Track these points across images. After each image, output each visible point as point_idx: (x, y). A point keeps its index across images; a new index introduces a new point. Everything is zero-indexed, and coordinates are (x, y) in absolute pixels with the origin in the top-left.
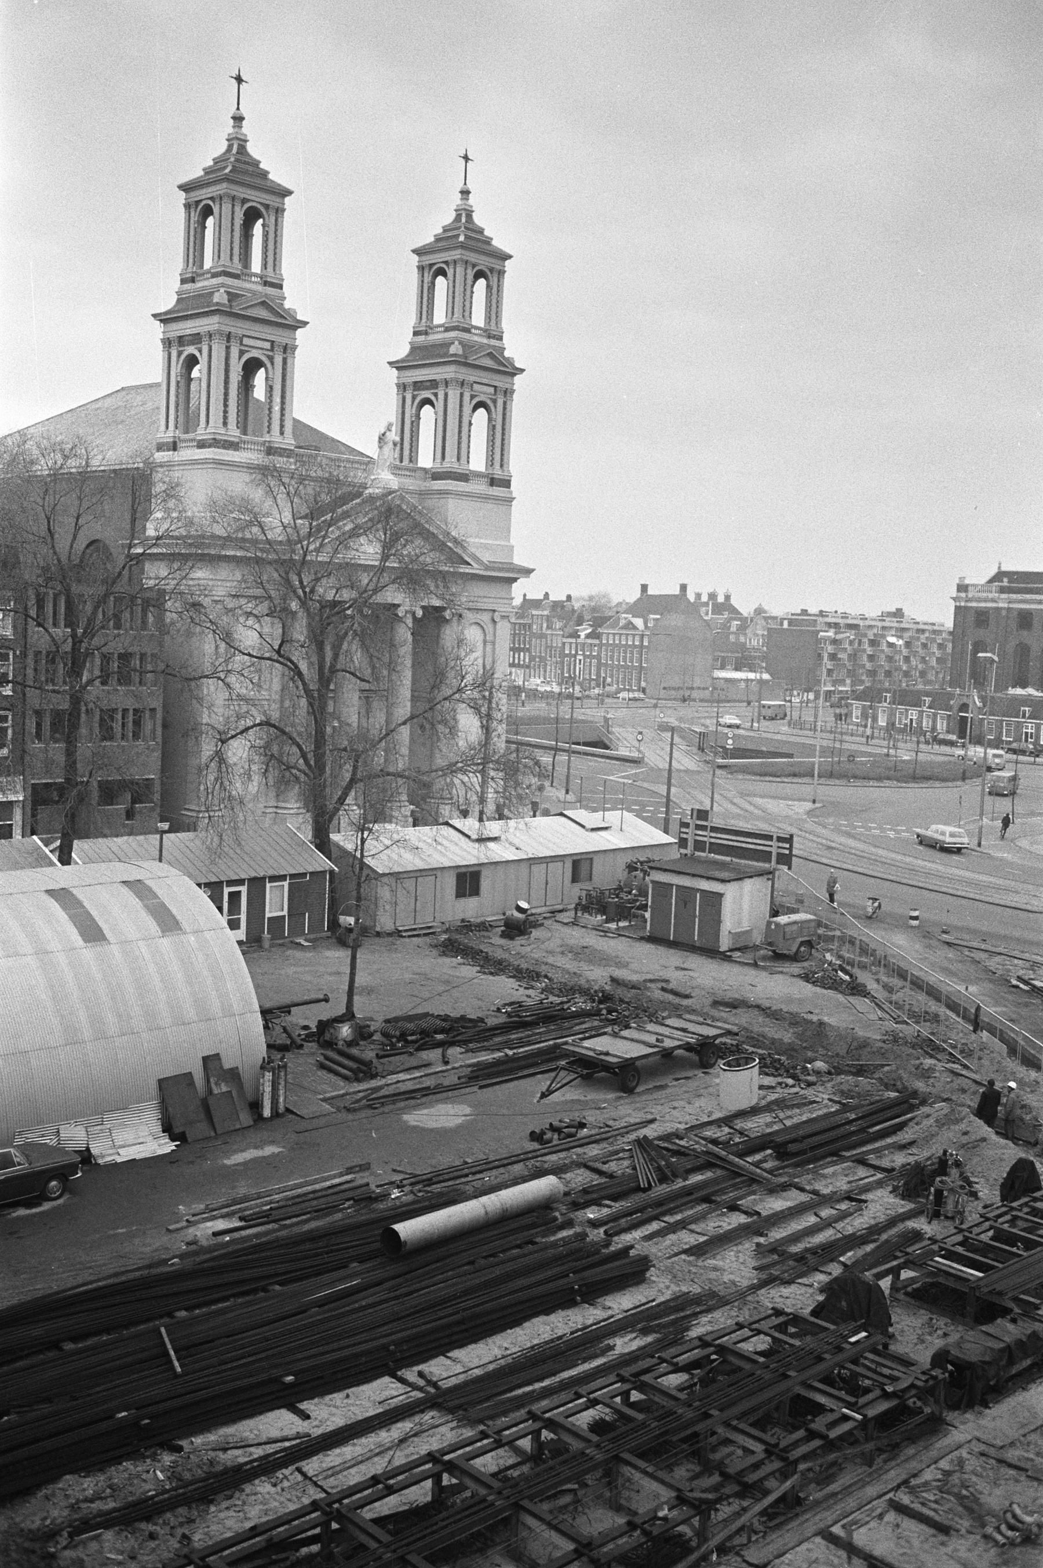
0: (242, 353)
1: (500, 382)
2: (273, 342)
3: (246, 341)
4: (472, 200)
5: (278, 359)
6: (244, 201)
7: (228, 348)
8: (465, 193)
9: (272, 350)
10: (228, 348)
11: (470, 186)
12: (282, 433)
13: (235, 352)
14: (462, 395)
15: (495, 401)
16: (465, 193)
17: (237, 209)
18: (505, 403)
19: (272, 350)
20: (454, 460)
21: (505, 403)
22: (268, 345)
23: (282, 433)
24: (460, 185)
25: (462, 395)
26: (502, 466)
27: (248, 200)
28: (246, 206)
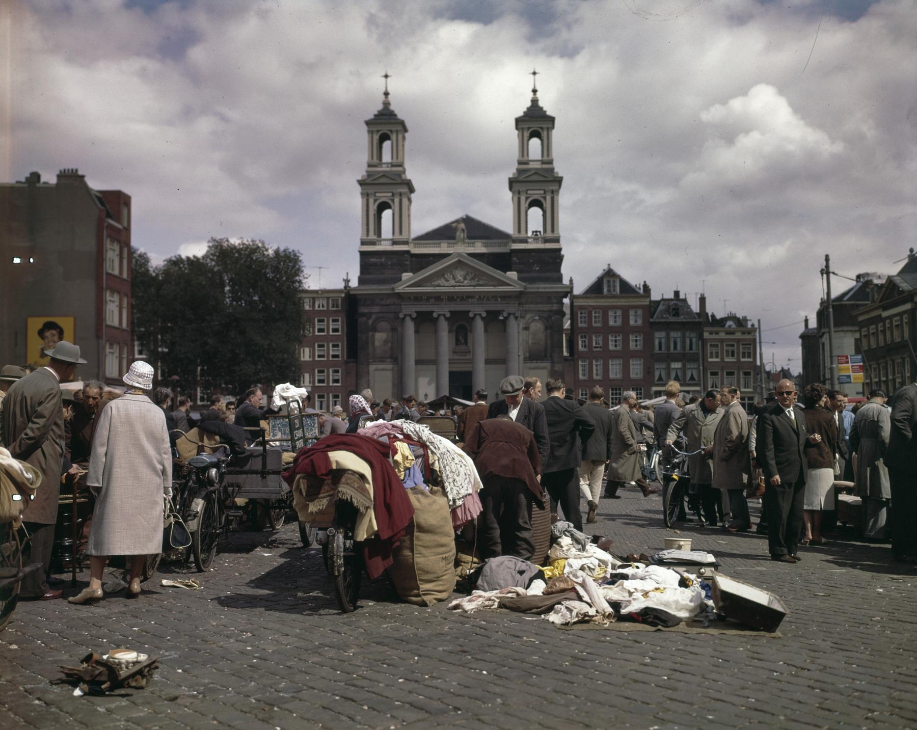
0: (375, 201)
4: (538, 95)
5: (397, 200)
6: (378, 131)
7: (368, 200)
8: (535, 91)
10: (368, 200)
11: (537, 88)
12: (401, 233)
13: (371, 201)
14: (519, 199)
15: (545, 198)
16: (535, 91)
23: (401, 233)
24: (532, 88)
25: (519, 199)
26: (553, 231)
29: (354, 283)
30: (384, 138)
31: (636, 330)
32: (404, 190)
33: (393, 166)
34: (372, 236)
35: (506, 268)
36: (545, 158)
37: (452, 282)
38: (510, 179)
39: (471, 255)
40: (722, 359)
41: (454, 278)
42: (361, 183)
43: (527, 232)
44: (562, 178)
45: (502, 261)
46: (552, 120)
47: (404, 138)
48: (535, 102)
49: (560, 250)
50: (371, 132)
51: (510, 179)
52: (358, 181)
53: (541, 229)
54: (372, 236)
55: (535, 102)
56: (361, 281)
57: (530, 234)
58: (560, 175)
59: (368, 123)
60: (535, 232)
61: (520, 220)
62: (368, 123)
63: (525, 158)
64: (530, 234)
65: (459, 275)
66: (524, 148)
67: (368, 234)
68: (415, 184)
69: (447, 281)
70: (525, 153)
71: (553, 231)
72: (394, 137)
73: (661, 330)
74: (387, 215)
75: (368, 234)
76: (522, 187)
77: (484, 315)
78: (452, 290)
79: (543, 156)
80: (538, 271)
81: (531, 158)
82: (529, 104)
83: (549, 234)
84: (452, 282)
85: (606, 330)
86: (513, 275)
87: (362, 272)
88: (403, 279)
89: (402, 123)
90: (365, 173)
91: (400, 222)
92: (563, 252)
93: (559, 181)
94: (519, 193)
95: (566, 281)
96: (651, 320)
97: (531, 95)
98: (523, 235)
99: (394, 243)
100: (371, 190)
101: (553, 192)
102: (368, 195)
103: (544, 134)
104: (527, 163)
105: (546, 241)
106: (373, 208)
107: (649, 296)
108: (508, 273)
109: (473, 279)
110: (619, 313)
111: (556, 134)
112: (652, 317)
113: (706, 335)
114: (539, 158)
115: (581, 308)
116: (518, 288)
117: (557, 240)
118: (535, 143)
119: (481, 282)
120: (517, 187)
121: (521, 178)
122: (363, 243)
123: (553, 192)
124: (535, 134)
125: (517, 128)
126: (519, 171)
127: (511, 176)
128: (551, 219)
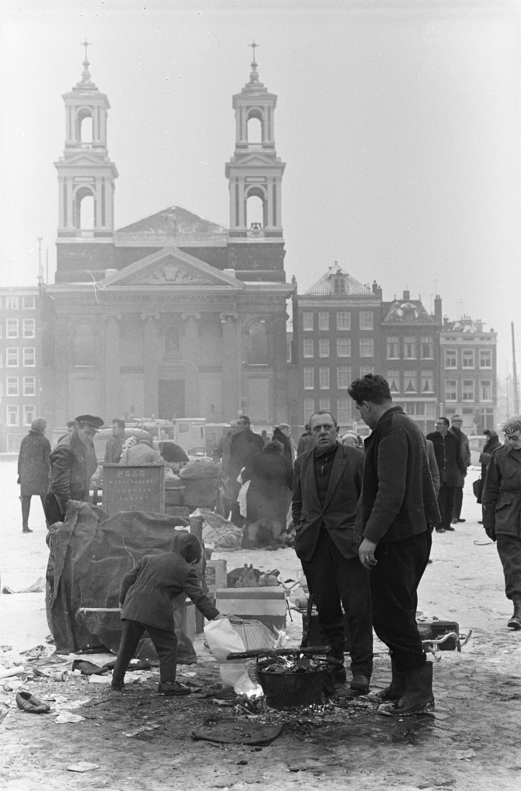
0: (74, 186)
1: (270, 174)
2: (94, 177)
3: (76, 179)
5: (99, 186)
6: (77, 107)
8: (254, 65)
9: (95, 181)
12: (103, 224)
14: (237, 187)
15: (266, 186)
16: (254, 65)
17: (73, 111)
18: (274, 187)
19: (95, 181)
20: (243, 225)
21: (274, 187)
22: (92, 179)
23: (103, 224)
25: (237, 187)
26: (275, 224)
27: (81, 106)
28: (78, 110)
29: (52, 281)
30: (83, 115)
31: (367, 335)
32: (107, 173)
33: (94, 147)
34: (71, 227)
35: (222, 265)
36: (267, 141)
37: (162, 280)
38: (227, 164)
39: (183, 249)
40: (460, 367)
41: (164, 275)
42: (58, 166)
43: (245, 225)
44: (285, 164)
45: (217, 257)
46: (274, 98)
47: (106, 115)
48: (254, 77)
49: (283, 244)
50: (69, 108)
51: (227, 164)
52: (54, 163)
53: (261, 221)
54: (71, 227)
55: (254, 77)
56: (58, 278)
57: (249, 226)
58: (283, 161)
59: (65, 97)
60: (255, 225)
61: (238, 211)
62: (65, 97)
63: (244, 141)
64: (249, 226)
65: (171, 271)
66: (242, 131)
67: (65, 225)
68: (119, 168)
69: (156, 278)
70: (244, 136)
71: (275, 224)
72: (95, 113)
73: (394, 335)
74: (87, 202)
75: (65, 225)
76: (242, 174)
77: (198, 317)
78: (163, 288)
79: (263, 139)
80: (258, 268)
81: (250, 141)
82: (248, 80)
83: (270, 227)
84: (162, 280)
85: (333, 336)
86: (230, 272)
87: (59, 268)
88: (107, 276)
89: (104, 98)
90: (62, 155)
91: (103, 211)
92: (285, 248)
93: (282, 167)
94: (237, 180)
95: (289, 280)
96: (383, 324)
97: (250, 70)
98: (241, 228)
99: (97, 235)
100: (66, 173)
101: (274, 180)
102: (65, 179)
103: (265, 115)
104: (245, 147)
105: (268, 235)
106: (71, 195)
107: (380, 298)
108: (225, 270)
109: (186, 276)
110: (348, 316)
111: (277, 114)
112: (382, 320)
113: (443, 341)
114: (259, 141)
115: (308, 310)
116: (237, 286)
117: (279, 234)
118: (254, 124)
119: (195, 281)
120: (234, 173)
121: (239, 163)
122: (60, 234)
123: (274, 180)
124: (255, 114)
125: (234, 107)
126: (238, 156)
127: (229, 161)
128: (272, 211)
